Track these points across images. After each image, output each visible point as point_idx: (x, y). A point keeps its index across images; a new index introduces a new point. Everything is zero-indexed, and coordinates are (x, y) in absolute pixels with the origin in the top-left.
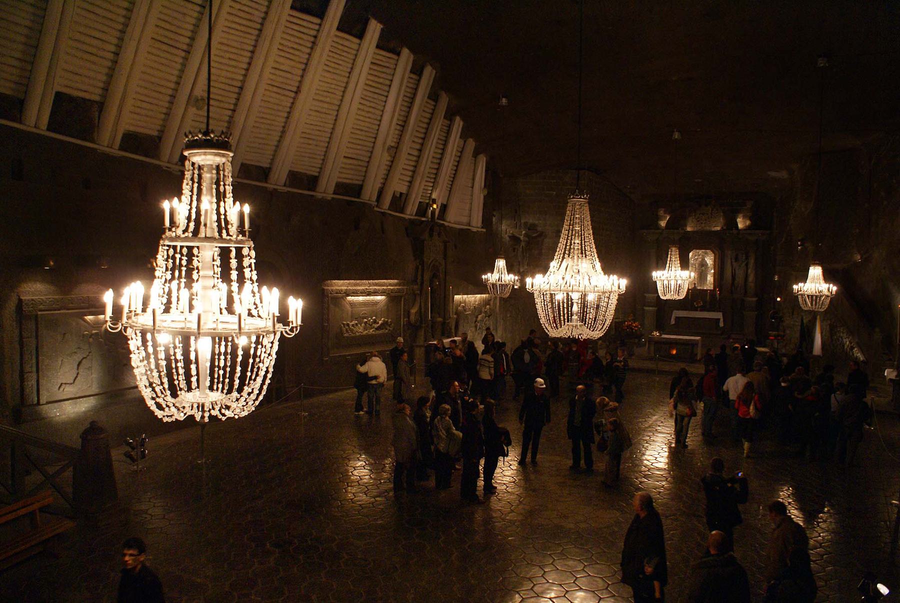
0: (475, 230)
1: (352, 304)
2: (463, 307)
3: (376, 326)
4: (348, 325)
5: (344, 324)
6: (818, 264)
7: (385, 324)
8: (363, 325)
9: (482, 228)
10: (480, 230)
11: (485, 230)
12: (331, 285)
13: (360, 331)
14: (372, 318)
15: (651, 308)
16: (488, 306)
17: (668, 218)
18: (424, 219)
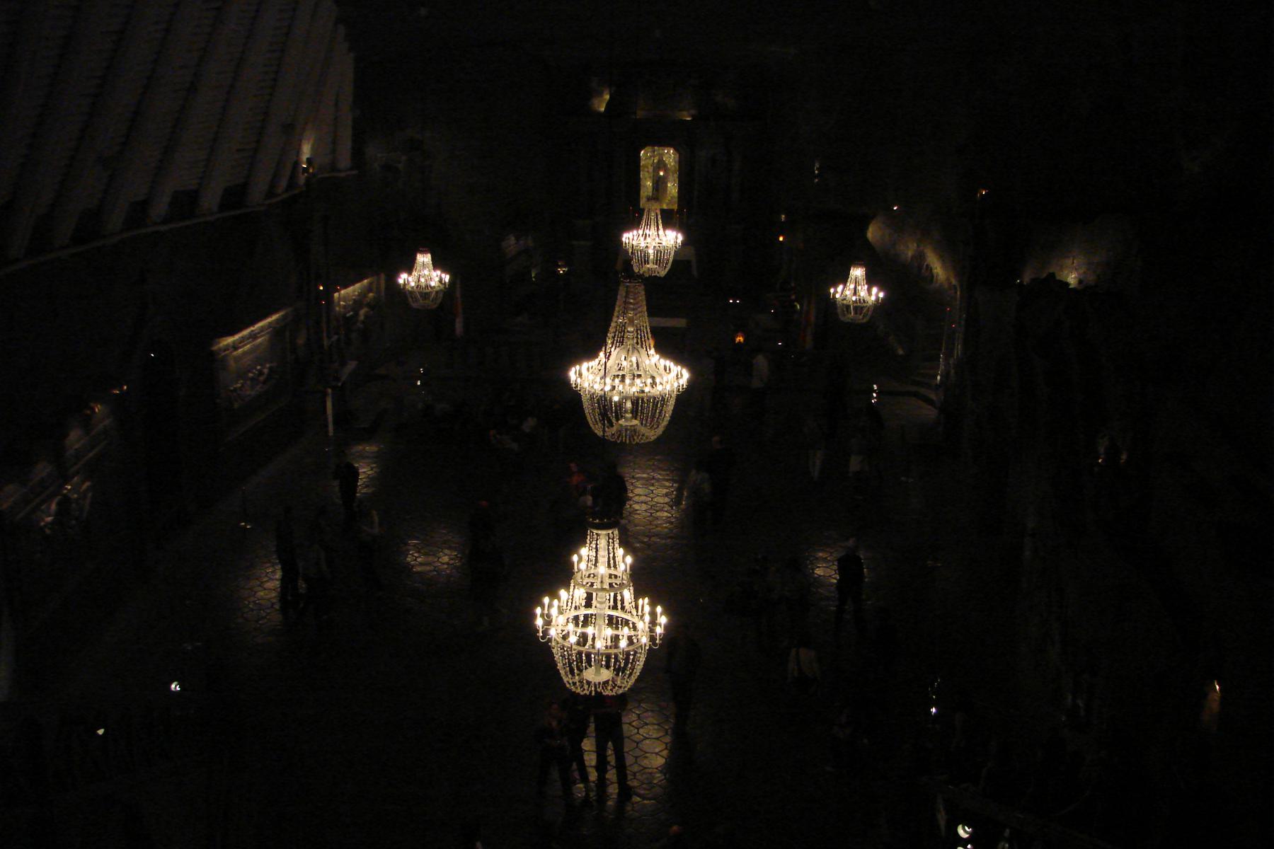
0: (343, 175)
1: (237, 359)
2: (344, 307)
3: (262, 378)
4: (235, 390)
5: (231, 391)
6: (860, 265)
7: (271, 369)
8: (249, 382)
9: (351, 169)
10: (349, 173)
11: (355, 172)
12: (219, 343)
13: (248, 393)
14: (255, 368)
15: (583, 243)
16: (371, 295)
17: (607, 97)
18: (296, 192)
